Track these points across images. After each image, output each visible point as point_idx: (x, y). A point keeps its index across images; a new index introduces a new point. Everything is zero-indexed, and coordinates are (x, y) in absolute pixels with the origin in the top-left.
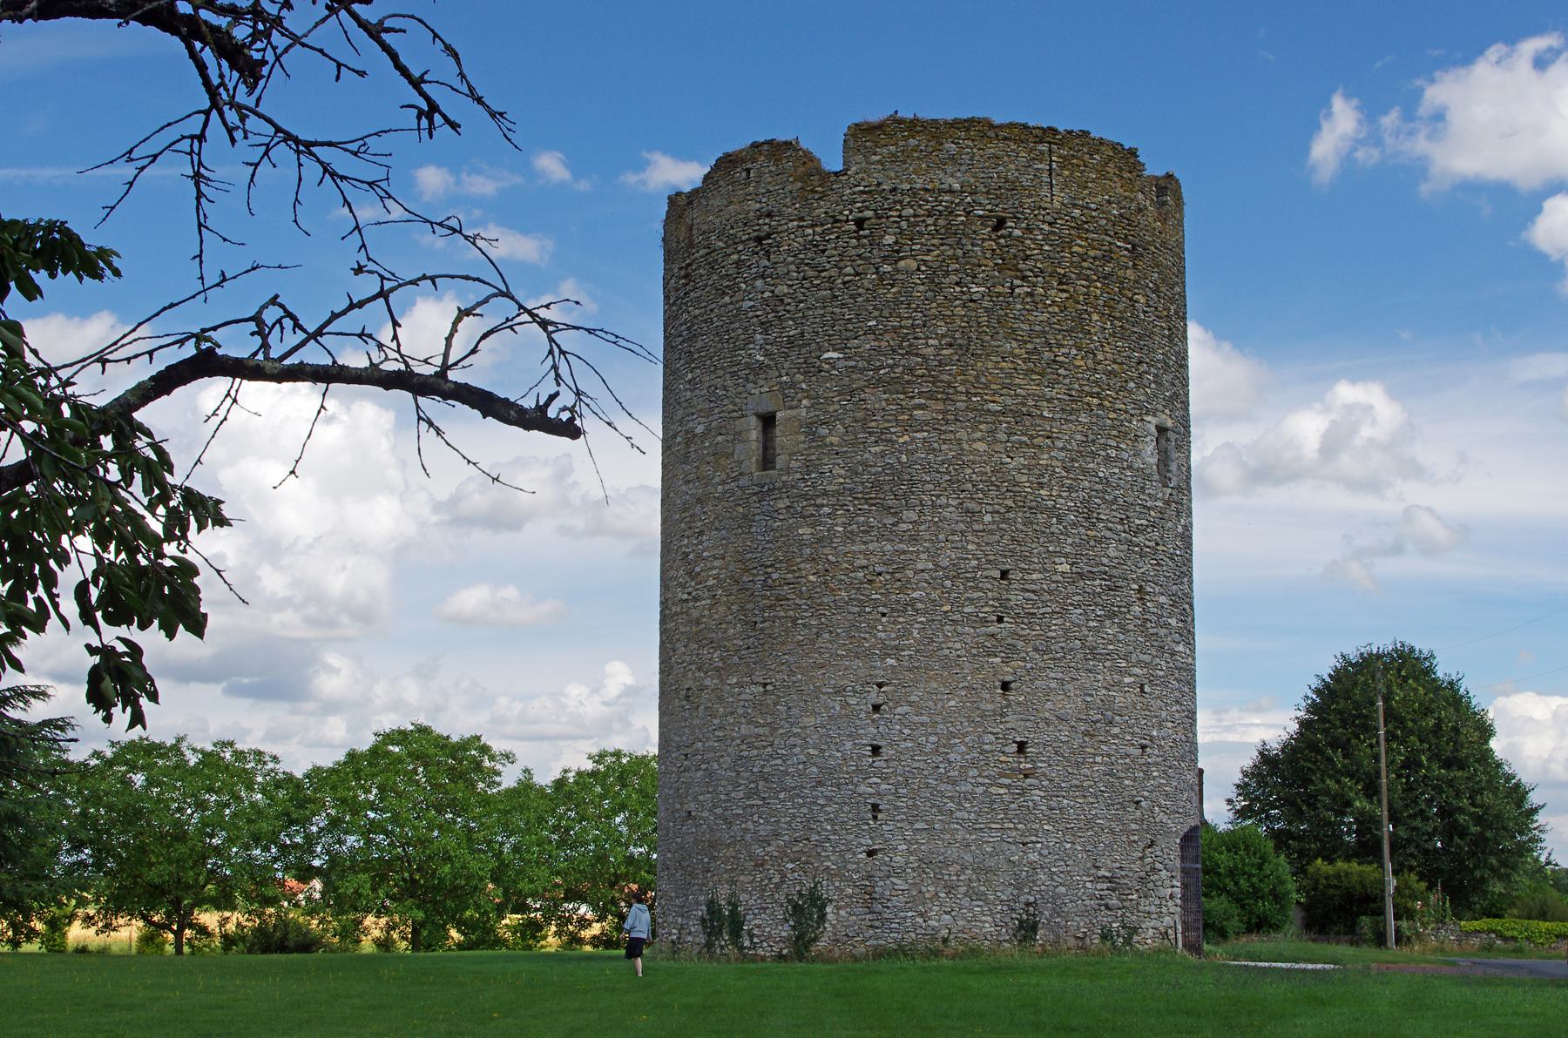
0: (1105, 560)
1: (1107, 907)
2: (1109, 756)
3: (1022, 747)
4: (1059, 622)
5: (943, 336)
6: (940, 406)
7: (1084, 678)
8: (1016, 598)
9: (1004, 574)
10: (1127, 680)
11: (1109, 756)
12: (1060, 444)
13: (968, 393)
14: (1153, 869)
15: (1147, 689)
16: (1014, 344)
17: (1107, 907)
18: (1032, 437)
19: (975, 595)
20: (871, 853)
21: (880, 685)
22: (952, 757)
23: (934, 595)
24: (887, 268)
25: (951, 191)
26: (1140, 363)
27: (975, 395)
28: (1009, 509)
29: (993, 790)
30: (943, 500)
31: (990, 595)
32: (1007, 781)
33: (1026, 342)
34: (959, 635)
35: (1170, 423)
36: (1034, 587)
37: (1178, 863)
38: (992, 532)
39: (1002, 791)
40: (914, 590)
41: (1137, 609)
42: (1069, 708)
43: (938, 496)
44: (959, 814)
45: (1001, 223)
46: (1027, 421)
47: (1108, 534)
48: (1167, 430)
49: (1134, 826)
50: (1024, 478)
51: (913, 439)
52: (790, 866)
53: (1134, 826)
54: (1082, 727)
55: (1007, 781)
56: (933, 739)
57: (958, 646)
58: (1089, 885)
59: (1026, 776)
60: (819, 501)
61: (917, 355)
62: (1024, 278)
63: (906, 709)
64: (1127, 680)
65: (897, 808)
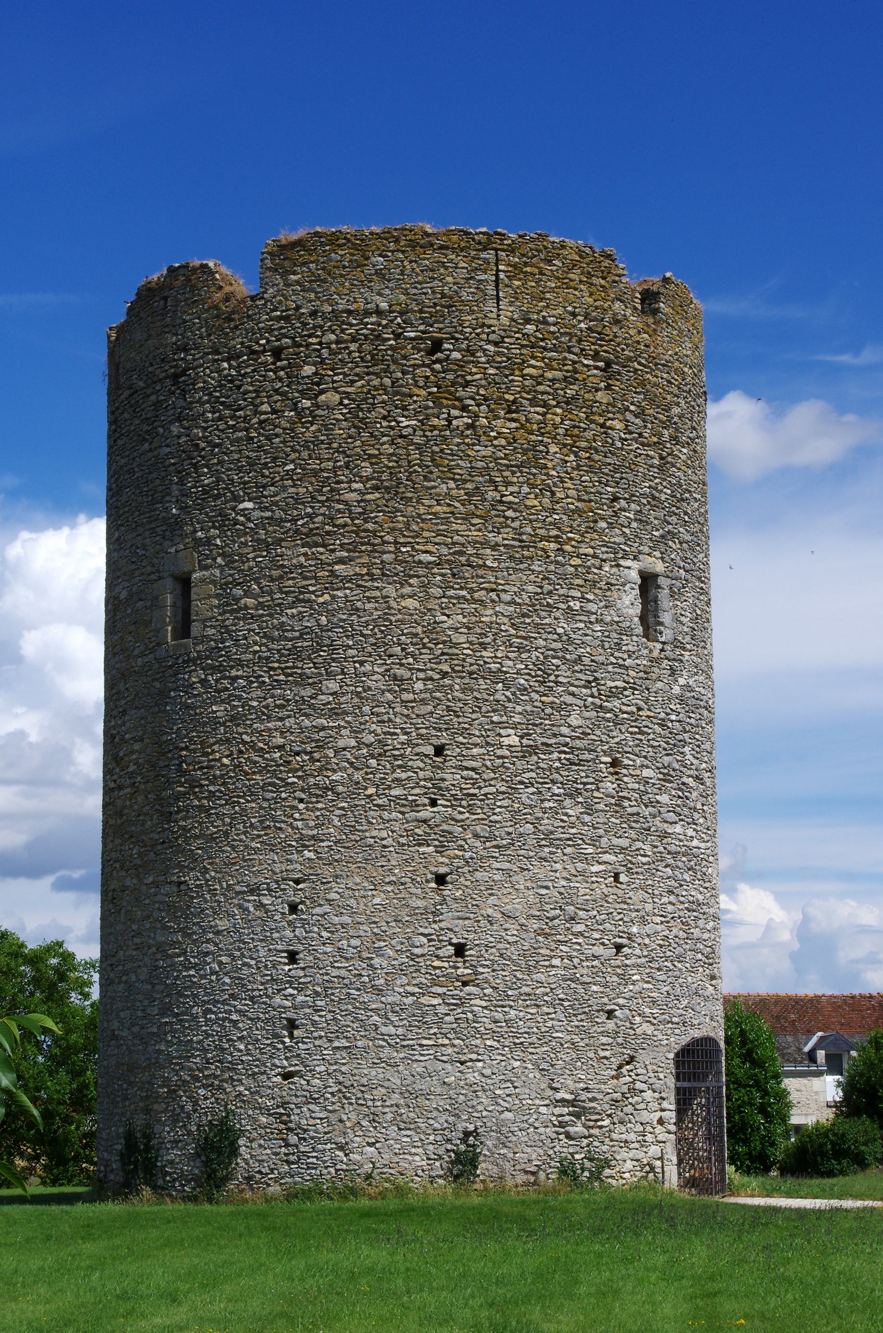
0: (565, 730)
1: (568, 1136)
2: (570, 958)
3: (460, 950)
4: (505, 803)
5: (368, 479)
6: (365, 560)
7: (538, 870)
8: (451, 777)
9: (439, 751)
10: (596, 868)
11: (570, 958)
12: (506, 597)
13: (396, 543)
14: (633, 1091)
15: (623, 878)
16: (452, 484)
17: (568, 1136)
18: (472, 591)
19: (404, 776)
20: (287, 1076)
21: (297, 882)
22: (376, 962)
23: (358, 776)
24: (307, 403)
25: (379, 312)
26: (615, 499)
27: (405, 545)
28: (444, 675)
29: (425, 1000)
30: (368, 667)
31: (421, 774)
32: (440, 990)
33: (465, 481)
34: (384, 821)
35: (660, 567)
36: (474, 764)
37: (671, 1082)
38: (423, 702)
39: (435, 1002)
40: (334, 771)
41: (609, 786)
42: (515, 905)
43: (362, 663)
44: (383, 1029)
45: (437, 346)
46: (468, 573)
47: (569, 699)
48: (656, 576)
49: (604, 1040)
50: (463, 639)
51: (333, 597)
52: (202, 1092)
53: (604, 1040)
54: (535, 925)
55: (440, 990)
56: (355, 942)
57: (384, 834)
58: (543, 1110)
59: (465, 984)
60: (234, 673)
61: (338, 501)
62: (464, 408)
63: (327, 908)
64: (596, 868)
65: (314, 1023)
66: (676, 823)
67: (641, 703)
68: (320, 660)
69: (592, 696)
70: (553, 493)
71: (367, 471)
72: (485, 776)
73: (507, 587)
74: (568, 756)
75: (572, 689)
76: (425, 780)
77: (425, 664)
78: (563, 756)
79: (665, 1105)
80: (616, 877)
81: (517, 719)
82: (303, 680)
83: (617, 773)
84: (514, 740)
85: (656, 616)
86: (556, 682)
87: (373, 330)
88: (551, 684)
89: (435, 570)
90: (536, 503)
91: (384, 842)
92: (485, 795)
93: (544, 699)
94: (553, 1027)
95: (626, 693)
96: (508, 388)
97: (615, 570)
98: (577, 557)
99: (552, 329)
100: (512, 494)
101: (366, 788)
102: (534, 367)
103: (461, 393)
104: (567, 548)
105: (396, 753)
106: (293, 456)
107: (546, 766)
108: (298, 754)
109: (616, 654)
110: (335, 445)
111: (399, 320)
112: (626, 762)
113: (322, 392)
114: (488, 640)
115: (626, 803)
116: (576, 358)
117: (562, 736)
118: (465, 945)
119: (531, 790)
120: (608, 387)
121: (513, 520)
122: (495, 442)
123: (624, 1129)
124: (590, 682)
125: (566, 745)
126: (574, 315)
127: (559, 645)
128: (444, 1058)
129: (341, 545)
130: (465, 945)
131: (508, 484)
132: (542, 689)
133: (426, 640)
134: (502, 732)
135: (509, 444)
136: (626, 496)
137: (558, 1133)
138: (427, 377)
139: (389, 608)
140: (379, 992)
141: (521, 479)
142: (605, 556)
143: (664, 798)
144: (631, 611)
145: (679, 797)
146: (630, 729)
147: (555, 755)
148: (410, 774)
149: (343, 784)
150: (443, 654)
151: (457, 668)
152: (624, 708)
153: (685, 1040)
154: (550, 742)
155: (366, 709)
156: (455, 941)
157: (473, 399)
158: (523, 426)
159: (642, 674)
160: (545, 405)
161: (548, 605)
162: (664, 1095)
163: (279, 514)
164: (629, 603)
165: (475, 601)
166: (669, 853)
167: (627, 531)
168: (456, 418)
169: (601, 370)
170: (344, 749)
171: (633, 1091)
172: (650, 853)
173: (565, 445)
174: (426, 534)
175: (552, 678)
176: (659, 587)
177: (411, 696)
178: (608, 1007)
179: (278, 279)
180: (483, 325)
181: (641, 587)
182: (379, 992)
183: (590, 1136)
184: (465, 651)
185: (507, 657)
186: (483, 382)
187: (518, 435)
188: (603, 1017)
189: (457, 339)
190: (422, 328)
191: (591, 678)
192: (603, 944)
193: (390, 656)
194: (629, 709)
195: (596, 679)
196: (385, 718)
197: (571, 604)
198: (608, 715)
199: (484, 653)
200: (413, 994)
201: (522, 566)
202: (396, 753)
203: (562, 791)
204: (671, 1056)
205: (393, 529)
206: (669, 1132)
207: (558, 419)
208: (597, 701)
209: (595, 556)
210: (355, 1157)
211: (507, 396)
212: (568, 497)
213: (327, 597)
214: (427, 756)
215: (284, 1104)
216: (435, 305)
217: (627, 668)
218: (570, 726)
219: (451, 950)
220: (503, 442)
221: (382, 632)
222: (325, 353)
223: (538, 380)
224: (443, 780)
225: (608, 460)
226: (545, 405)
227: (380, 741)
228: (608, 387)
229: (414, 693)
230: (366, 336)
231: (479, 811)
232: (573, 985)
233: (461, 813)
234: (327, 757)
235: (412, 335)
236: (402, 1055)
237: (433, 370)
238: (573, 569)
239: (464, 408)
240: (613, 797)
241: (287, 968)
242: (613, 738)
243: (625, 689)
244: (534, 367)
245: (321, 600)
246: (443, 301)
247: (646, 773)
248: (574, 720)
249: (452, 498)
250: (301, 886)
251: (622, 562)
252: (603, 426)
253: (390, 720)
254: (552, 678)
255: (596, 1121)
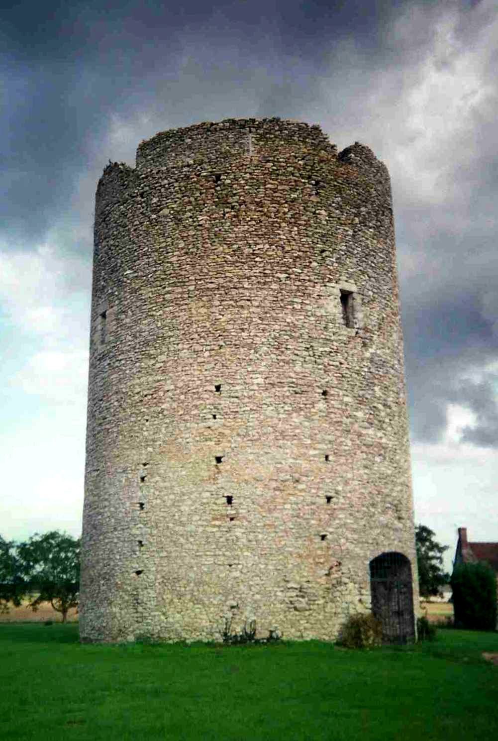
0: (292, 375)
1: (296, 609)
2: (297, 504)
3: (229, 500)
4: (256, 415)
5: (182, 249)
6: (180, 290)
7: (273, 451)
8: (224, 403)
9: (218, 388)
10: (312, 452)
11: (297, 504)
12: (256, 304)
13: (196, 280)
14: (340, 583)
15: (330, 458)
16: (225, 246)
17: (296, 609)
18: (236, 301)
19: (198, 403)
20: (139, 573)
21: (145, 465)
22: (182, 508)
23: (175, 405)
24: (154, 216)
25: (188, 166)
26: (323, 251)
27: (200, 280)
28: (221, 347)
29: (209, 529)
30: (180, 346)
31: (208, 402)
32: (217, 523)
33: (233, 244)
34: (188, 429)
35: (353, 288)
36: (236, 394)
37: (368, 578)
38: (209, 363)
39: (215, 530)
40: (163, 403)
41: (321, 405)
42: (263, 473)
43: (178, 344)
44: (186, 546)
45: (218, 178)
46: (234, 292)
47: (294, 357)
48: (351, 293)
49: (319, 552)
50: (230, 327)
51: (164, 312)
52: (102, 582)
53: (319, 552)
54: (274, 484)
55: (217, 523)
56: (172, 497)
57: (187, 436)
58: (279, 594)
59: (232, 519)
60: (120, 358)
61: (168, 262)
62: (233, 208)
63: (158, 478)
64: (312, 452)
65: (151, 543)
66: (369, 428)
67: (343, 361)
68: (157, 345)
69: (310, 356)
70: (283, 248)
71: (182, 245)
72: (243, 401)
73: (256, 298)
74: (294, 389)
75: (296, 352)
76: (210, 404)
77: (210, 342)
78: (291, 389)
79: (364, 591)
80: (327, 457)
81: (262, 369)
82: (150, 356)
83: (326, 399)
84: (261, 381)
85: (353, 315)
86: (286, 349)
87: (185, 175)
88: (283, 349)
89: (216, 292)
90: (273, 253)
91: (188, 440)
92: (244, 411)
93: (279, 357)
94: (285, 544)
95: (332, 354)
96: (256, 195)
97: (324, 288)
98: (299, 281)
99: (282, 164)
100: (259, 249)
101: (178, 412)
102: (272, 184)
103: (230, 200)
104: (293, 276)
105: (194, 391)
106: (148, 243)
107: (280, 395)
108: (146, 396)
109: (325, 333)
110: (166, 235)
111: (199, 168)
112: (332, 392)
113: (161, 209)
114: (245, 327)
115: (332, 416)
116: (297, 179)
117: (290, 377)
118: (232, 497)
119: (271, 408)
120: (317, 194)
121: (260, 262)
122: (249, 223)
123: (334, 605)
124: (308, 348)
125: (293, 383)
126: (296, 157)
127: (288, 328)
128: (219, 563)
129: (169, 284)
130: (232, 497)
131: (256, 244)
132: (277, 352)
133: (211, 329)
134: (254, 376)
135: (257, 223)
136: (331, 249)
137: (289, 608)
138: (213, 194)
139: (192, 314)
140: (182, 524)
141: (264, 241)
142: (316, 281)
143: (360, 414)
144: (335, 311)
145: (371, 414)
146: (336, 375)
147: (286, 389)
148: (202, 402)
149: (167, 410)
150: (220, 336)
151: (228, 343)
152: (331, 363)
153: (377, 553)
154: (282, 381)
155: (180, 369)
156: (226, 495)
157: (237, 202)
158: (265, 214)
159: (343, 345)
160: (279, 203)
161: (281, 307)
162: (362, 586)
163: (140, 274)
164: (333, 307)
165: (238, 307)
166: (364, 445)
167: (331, 268)
168: (227, 213)
169: (313, 185)
170: (168, 391)
171: (340, 583)
172: (350, 445)
173: (291, 223)
174: (211, 273)
175: (284, 346)
176: (354, 299)
177: (203, 360)
178: (322, 534)
179: (144, 160)
180: (243, 165)
181: (341, 298)
182: (182, 524)
183: (310, 610)
184: (233, 334)
185: (257, 336)
186: (243, 193)
187: (262, 219)
188: (318, 540)
189: (228, 173)
190: (210, 170)
191: (309, 346)
192: (319, 496)
193: (192, 339)
194: (334, 363)
195: (311, 346)
196: (189, 373)
197: (295, 306)
198: (320, 367)
199: (243, 334)
200: (202, 526)
201: (265, 287)
202: (194, 391)
203: (290, 409)
204: (368, 562)
205: (194, 273)
206: (367, 608)
207: (286, 210)
208: (313, 359)
209: (309, 281)
210: (171, 620)
211: (256, 200)
212: (292, 250)
213: (161, 312)
214: (211, 391)
215: (136, 589)
216: (217, 158)
217: (332, 341)
218: (295, 372)
219: (225, 500)
220: (254, 223)
221: (188, 327)
222: (163, 190)
223: (275, 190)
224: (220, 404)
225: (317, 231)
226: (279, 203)
227: (186, 385)
228: (317, 194)
229: (204, 358)
230: (182, 178)
231: (240, 420)
232: (299, 520)
233: (229, 422)
234: (159, 396)
235: (205, 174)
236: (196, 561)
237: (215, 190)
238: (296, 288)
239: (233, 208)
240: (324, 412)
241: (139, 512)
242: (324, 379)
243: (331, 352)
244: (272, 184)
245: (158, 314)
246: (221, 156)
247: (346, 399)
248: (298, 368)
249: (226, 254)
250: (146, 467)
251: (328, 284)
252: (314, 213)
253: (191, 374)
254: (284, 346)
255: (315, 600)
